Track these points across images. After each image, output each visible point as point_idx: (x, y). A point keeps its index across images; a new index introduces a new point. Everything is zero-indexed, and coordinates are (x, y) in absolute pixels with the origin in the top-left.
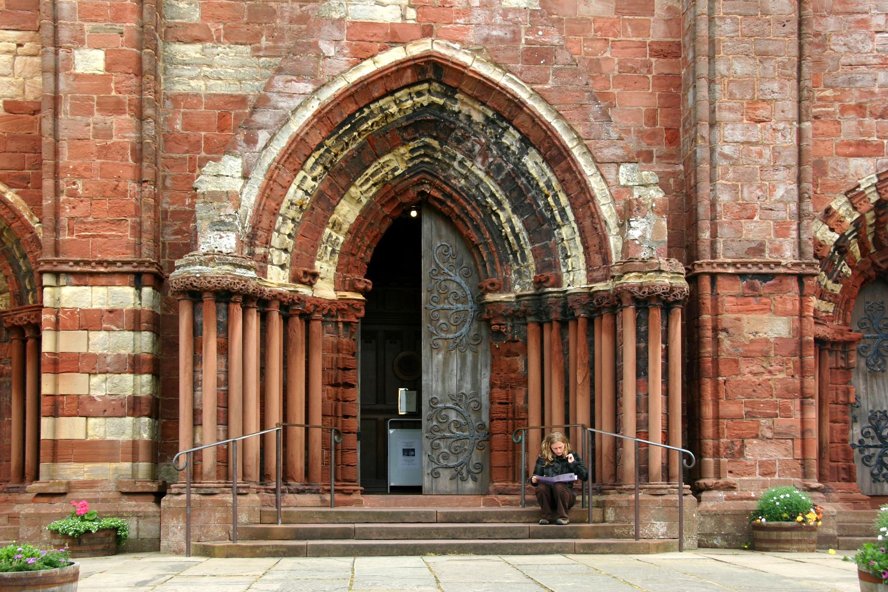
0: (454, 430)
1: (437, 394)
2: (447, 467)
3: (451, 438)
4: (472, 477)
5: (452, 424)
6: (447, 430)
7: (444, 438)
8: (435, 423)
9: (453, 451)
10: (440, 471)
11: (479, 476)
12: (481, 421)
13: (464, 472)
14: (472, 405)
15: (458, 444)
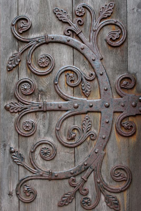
0: (68, 93)
1: (28, 10)
2: (52, 178)
3: (60, 109)
4: (107, 199)
5: (63, 79)
6: (53, 93)
7: (43, 110)
8: (24, 76)
9: (65, 139)
10: (36, 185)
11: (123, 199)
12: (127, 69)
13: (90, 186)
14: (106, 33)
15: (78, 125)
